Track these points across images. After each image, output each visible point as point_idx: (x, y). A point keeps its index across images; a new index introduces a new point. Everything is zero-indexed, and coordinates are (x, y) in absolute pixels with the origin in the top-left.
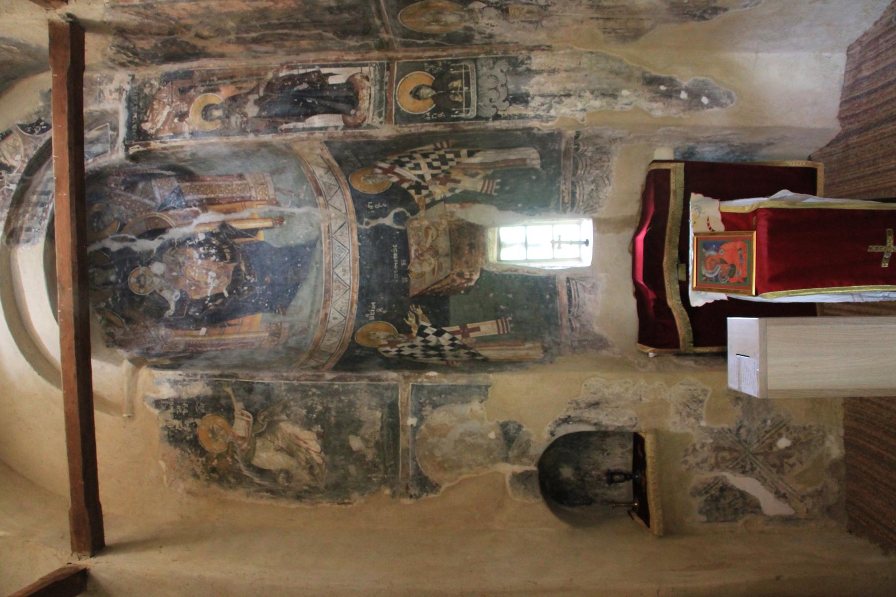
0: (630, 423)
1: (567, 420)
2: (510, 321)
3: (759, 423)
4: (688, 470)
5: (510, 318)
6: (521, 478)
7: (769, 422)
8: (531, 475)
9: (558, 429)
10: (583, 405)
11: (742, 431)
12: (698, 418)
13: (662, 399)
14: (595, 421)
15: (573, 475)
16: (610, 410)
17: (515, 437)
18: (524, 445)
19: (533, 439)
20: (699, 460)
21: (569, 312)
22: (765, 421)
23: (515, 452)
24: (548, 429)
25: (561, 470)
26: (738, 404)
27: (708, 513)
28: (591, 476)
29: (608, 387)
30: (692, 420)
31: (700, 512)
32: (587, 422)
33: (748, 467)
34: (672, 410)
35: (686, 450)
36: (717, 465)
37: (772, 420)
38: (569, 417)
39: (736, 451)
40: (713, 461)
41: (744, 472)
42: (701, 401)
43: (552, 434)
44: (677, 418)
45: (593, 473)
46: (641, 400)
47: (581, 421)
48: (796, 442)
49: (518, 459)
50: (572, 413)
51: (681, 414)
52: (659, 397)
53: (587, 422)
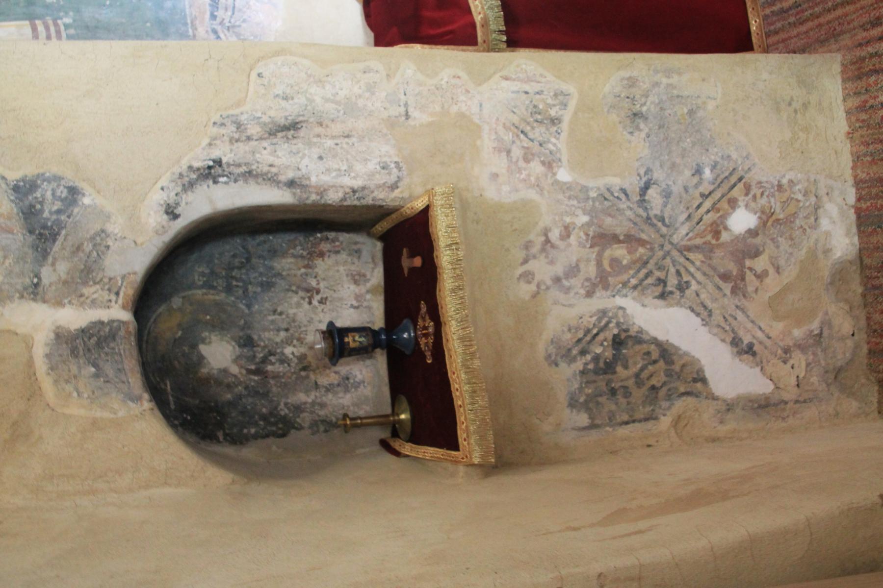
0: (381, 178)
1: (211, 172)
2: (67, 26)
3: (688, 173)
4: (535, 295)
5: (68, 20)
6: (84, 346)
7: (707, 173)
8: (113, 336)
9: (190, 197)
10: (254, 130)
11: (652, 193)
12: (549, 165)
13: (462, 115)
14: (290, 175)
15: (236, 361)
16: (329, 143)
17: (60, 225)
18: (88, 247)
19: (115, 227)
20: (559, 269)
21: (213, 17)
22: (698, 171)
23: (63, 268)
24: (158, 197)
25: (203, 349)
26: (638, 128)
27: (589, 405)
28: (283, 360)
29: (320, 82)
30: (536, 168)
31: (573, 404)
32: (271, 179)
33: (672, 281)
34: (487, 142)
35: (527, 246)
36: (601, 282)
37: (713, 168)
38: (218, 162)
39: (642, 243)
40: (591, 270)
41: (662, 296)
42: (555, 121)
43: (171, 213)
44: (500, 164)
45: (288, 350)
46: (407, 116)
47: (249, 175)
48: (767, 218)
49: (71, 290)
50: (226, 153)
51: (509, 152)
52: (454, 109)
53: (271, 179)
